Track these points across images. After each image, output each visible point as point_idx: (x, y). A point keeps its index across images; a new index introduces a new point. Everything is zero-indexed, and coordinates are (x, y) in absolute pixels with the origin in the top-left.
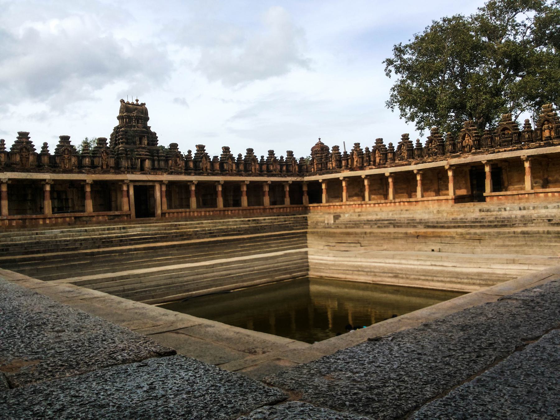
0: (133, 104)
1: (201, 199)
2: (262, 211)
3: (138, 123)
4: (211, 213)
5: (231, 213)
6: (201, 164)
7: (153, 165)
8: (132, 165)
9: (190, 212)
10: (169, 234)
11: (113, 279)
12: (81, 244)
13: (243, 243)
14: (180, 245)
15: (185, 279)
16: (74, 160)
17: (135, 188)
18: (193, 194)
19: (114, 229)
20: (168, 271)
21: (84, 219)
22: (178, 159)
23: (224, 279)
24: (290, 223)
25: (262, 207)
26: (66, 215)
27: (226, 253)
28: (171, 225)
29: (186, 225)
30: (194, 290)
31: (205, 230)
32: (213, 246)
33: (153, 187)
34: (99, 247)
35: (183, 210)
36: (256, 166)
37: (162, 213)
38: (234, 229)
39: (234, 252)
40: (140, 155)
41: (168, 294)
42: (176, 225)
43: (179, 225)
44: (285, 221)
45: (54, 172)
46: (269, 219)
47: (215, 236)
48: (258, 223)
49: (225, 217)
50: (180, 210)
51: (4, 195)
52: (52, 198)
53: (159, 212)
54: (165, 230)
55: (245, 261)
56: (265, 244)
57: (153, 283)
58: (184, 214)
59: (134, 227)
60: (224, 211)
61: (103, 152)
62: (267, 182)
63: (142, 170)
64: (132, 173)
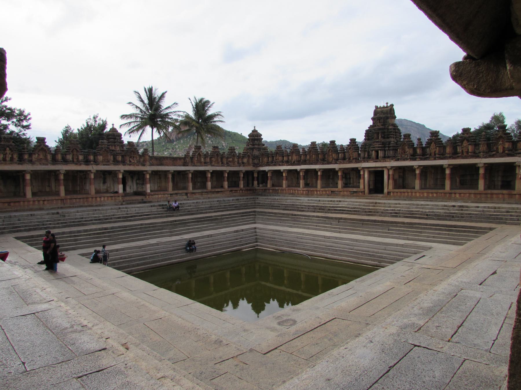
0: (384, 107)
1: (458, 180)
2: (506, 196)
3: (380, 122)
4: (435, 195)
5: (460, 196)
6: (428, 150)
7: (385, 154)
8: (368, 155)
9: (412, 193)
10: (364, 209)
11: (273, 230)
12: (309, 208)
13: (397, 226)
14: (345, 219)
15: (302, 240)
16: (334, 155)
17: (370, 173)
18: (418, 176)
19: (334, 201)
20: (300, 233)
21: (336, 192)
22: (406, 147)
23: (323, 249)
24: (511, 216)
25: (505, 192)
26: (326, 189)
27: (368, 231)
28: (372, 203)
29: (385, 203)
30: (297, 249)
31: (395, 210)
32: (367, 224)
33: (383, 171)
34: (314, 212)
35: (405, 190)
36: (505, 145)
37: (388, 192)
38: (426, 212)
39: (376, 232)
40: (374, 148)
41: (283, 246)
42: (376, 203)
43: (379, 203)
44: (508, 212)
45: (323, 164)
46: (485, 207)
47: (396, 216)
48: (462, 210)
49: (450, 199)
50: (402, 190)
51: (302, 177)
52: (343, 178)
53: (386, 191)
54: (364, 206)
55: (357, 241)
56: (417, 232)
57: (284, 238)
58: (406, 194)
59: (346, 202)
60: (451, 193)
61: (350, 149)
62: (515, 163)
63: (377, 159)
64: (368, 162)
